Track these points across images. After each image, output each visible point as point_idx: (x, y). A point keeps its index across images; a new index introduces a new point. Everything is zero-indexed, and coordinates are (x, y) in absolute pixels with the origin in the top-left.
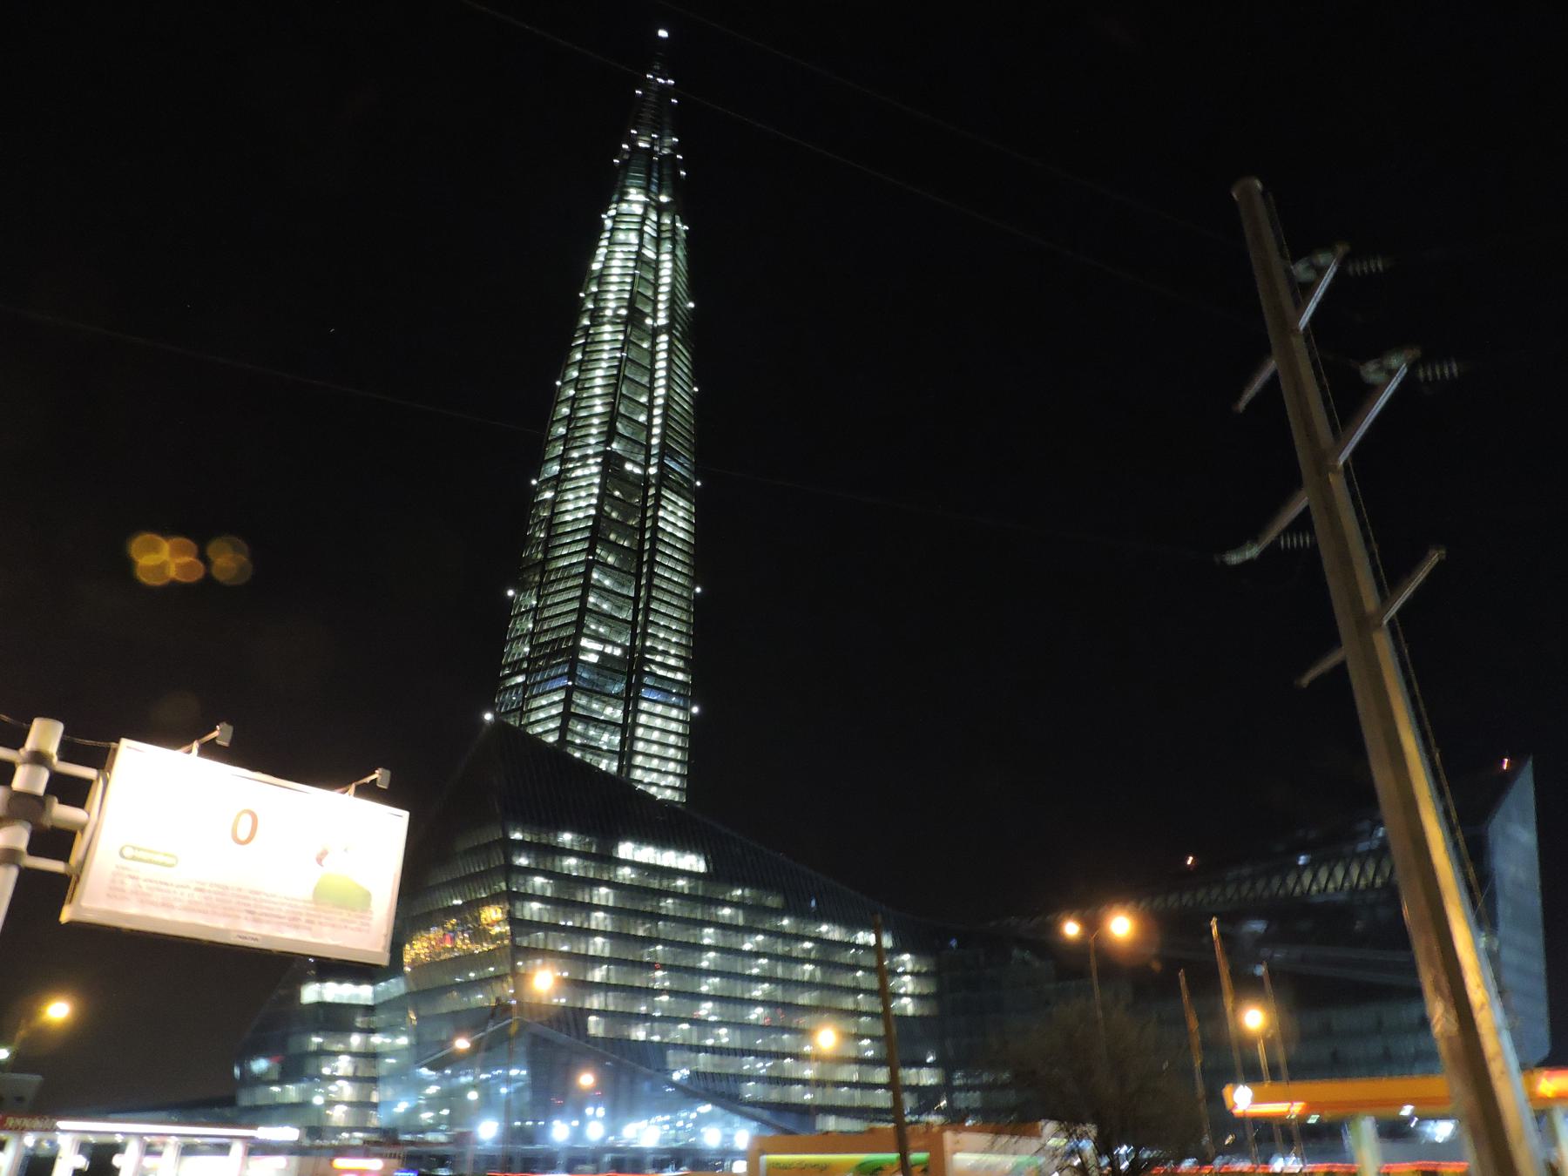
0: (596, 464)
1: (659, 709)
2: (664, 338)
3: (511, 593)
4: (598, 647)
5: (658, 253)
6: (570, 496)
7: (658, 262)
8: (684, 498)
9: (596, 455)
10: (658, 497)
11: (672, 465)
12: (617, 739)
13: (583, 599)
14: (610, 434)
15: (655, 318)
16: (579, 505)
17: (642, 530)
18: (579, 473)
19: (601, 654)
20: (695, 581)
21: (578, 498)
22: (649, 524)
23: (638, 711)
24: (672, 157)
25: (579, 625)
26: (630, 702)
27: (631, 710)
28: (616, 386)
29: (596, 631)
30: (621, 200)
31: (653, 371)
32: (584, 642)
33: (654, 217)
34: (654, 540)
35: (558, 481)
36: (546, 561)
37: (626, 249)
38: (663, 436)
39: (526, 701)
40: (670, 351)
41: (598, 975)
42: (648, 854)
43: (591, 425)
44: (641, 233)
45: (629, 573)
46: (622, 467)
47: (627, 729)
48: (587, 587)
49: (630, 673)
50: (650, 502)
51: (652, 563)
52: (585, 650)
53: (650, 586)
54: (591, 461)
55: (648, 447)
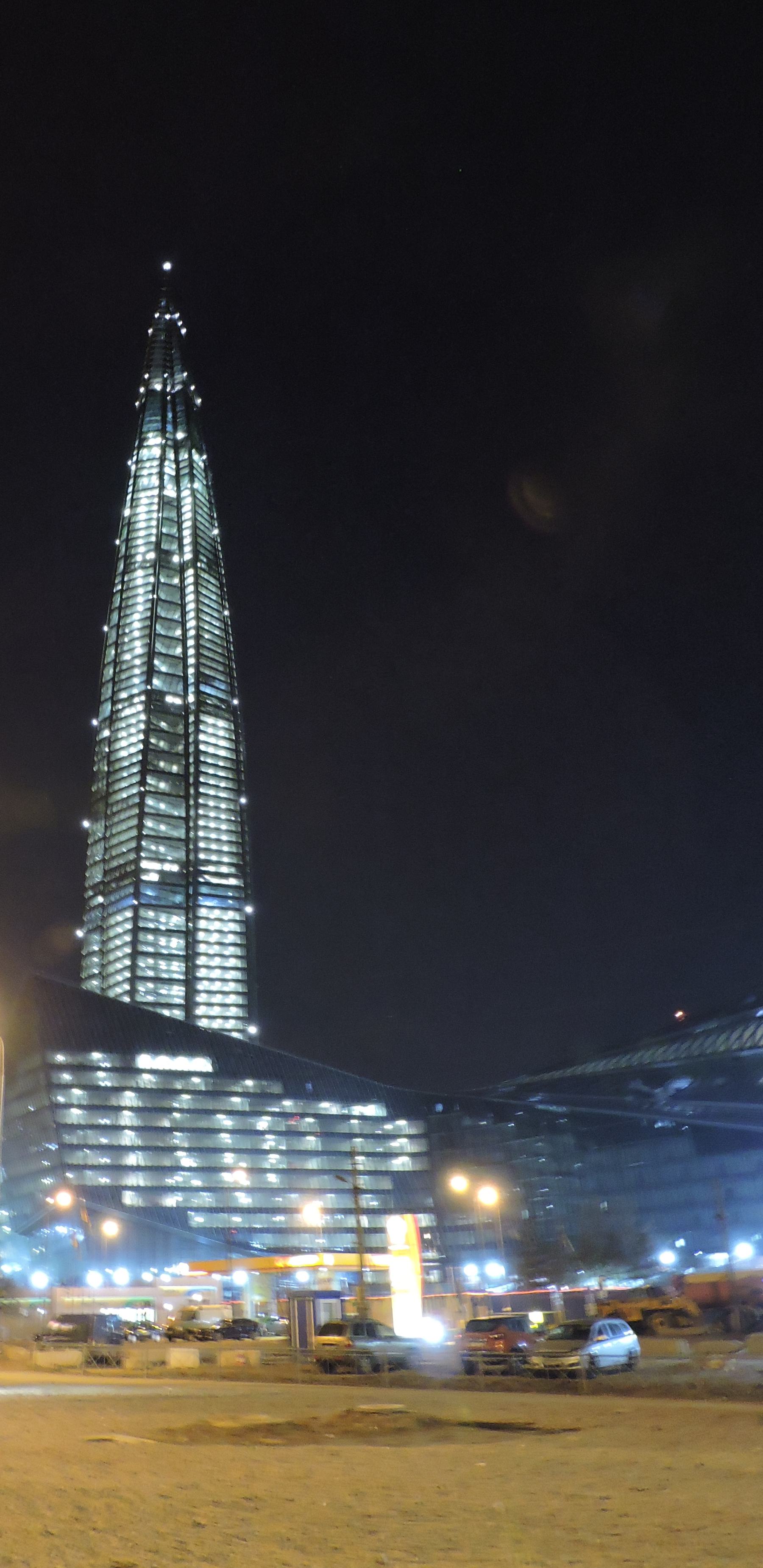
0: (141, 702)
1: (217, 913)
2: (190, 572)
3: (86, 824)
4: (157, 866)
5: (179, 491)
6: (123, 734)
7: (179, 499)
9: (139, 694)
10: (198, 722)
11: (208, 690)
12: (182, 942)
13: (140, 826)
14: (150, 672)
15: (181, 553)
16: (129, 742)
17: (187, 754)
18: (127, 712)
19: (161, 873)
20: (238, 792)
21: (130, 735)
22: (192, 749)
23: (197, 918)
24: (185, 391)
25: (138, 849)
26: (190, 909)
28: (151, 627)
29: (157, 852)
30: (141, 447)
31: (183, 606)
32: (144, 864)
33: (171, 455)
34: (198, 762)
35: (112, 720)
36: (108, 794)
37: (149, 493)
38: (197, 666)
39: (103, 919)
40: (196, 584)
41: (132, 1159)
43: (133, 667)
44: (161, 475)
45: (181, 797)
46: (163, 701)
47: (189, 935)
48: (142, 815)
49: (187, 885)
50: (191, 729)
51: (197, 784)
52: (147, 871)
54: (136, 700)
55: (185, 678)
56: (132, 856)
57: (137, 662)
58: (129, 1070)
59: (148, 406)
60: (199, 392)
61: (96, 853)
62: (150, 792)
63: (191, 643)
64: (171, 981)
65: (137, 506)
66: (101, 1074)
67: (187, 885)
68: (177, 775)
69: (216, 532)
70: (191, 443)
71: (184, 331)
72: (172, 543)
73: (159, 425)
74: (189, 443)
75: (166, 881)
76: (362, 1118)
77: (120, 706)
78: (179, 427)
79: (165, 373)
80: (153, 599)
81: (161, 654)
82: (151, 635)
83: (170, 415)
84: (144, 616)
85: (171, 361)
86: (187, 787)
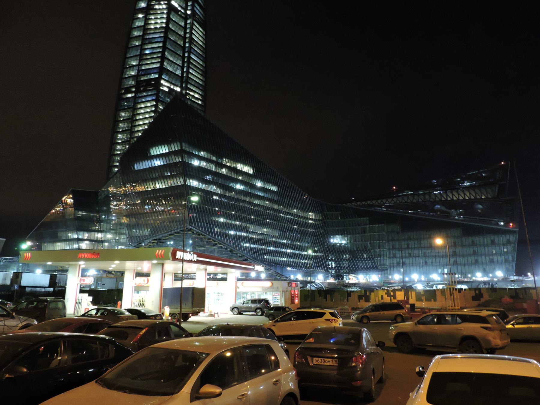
10: (192, 24)
32: (162, 82)
39: (136, 103)
53: (189, 62)
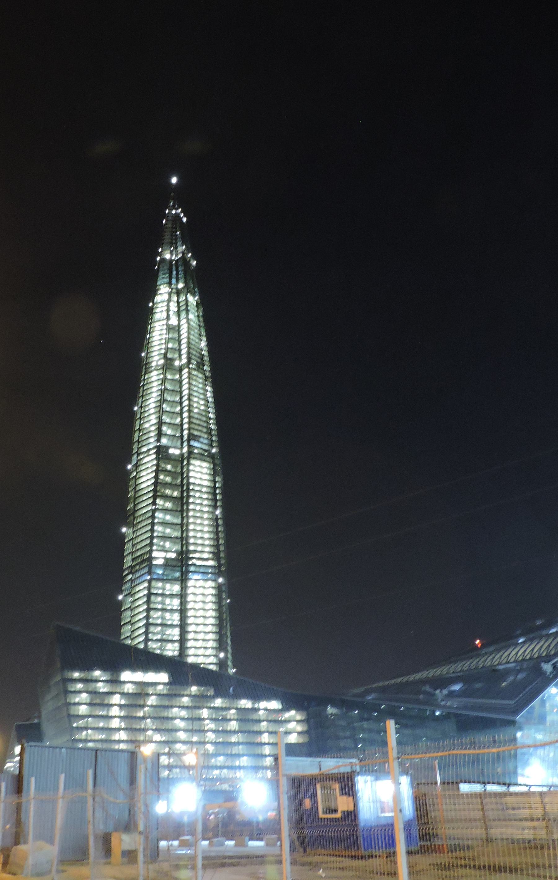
1: (201, 583)
2: (186, 370)
4: (163, 554)
5: (179, 321)
7: (179, 326)
8: (205, 461)
10: (188, 464)
13: (152, 530)
14: (160, 434)
17: (182, 485)
19: (166, 559)
22: (185, 482)
24: (183, 258)
25: (151, 544)
26: (183, 580)
27: (184, 588)
31: (181, 392)
33: (175, 298)
34: (188, 490)
36: (135, 511)
38: (189, 429)
39: (132, 588)
40: (189, 377)
42: (139, 676)
44: (168, 311)
47: (183, 596)
49: (181, 565)
51: (188, 503)
52: (156, 558)
55: (182, 437)
56: (148, 549)
57: (153, 428)
58: (115, 681)
59: (160, 269)
60: (194, 257)
61: (128, 547)
62: (158, 509)
63: (186, 415)
64: (172, 626)
65: (153, 332)
66: (100, 684)
67: (181, 565)
68: (176, 498)
69: (203, 344)
70: (187, 290)
71: (185, 220)
72: (174, 353)
73: (167, 280)
74: (186, 290)
75: (168, 564)
76: (266, 709)
77: (142, 456)
78: (180, 281)
79: (171, 247)
80: (161, 389)
81: (166, 423)
82: (161, 411)
83: (174, 273)
84: (156, 400)
85: (176, 239)
86: (182, 504)
